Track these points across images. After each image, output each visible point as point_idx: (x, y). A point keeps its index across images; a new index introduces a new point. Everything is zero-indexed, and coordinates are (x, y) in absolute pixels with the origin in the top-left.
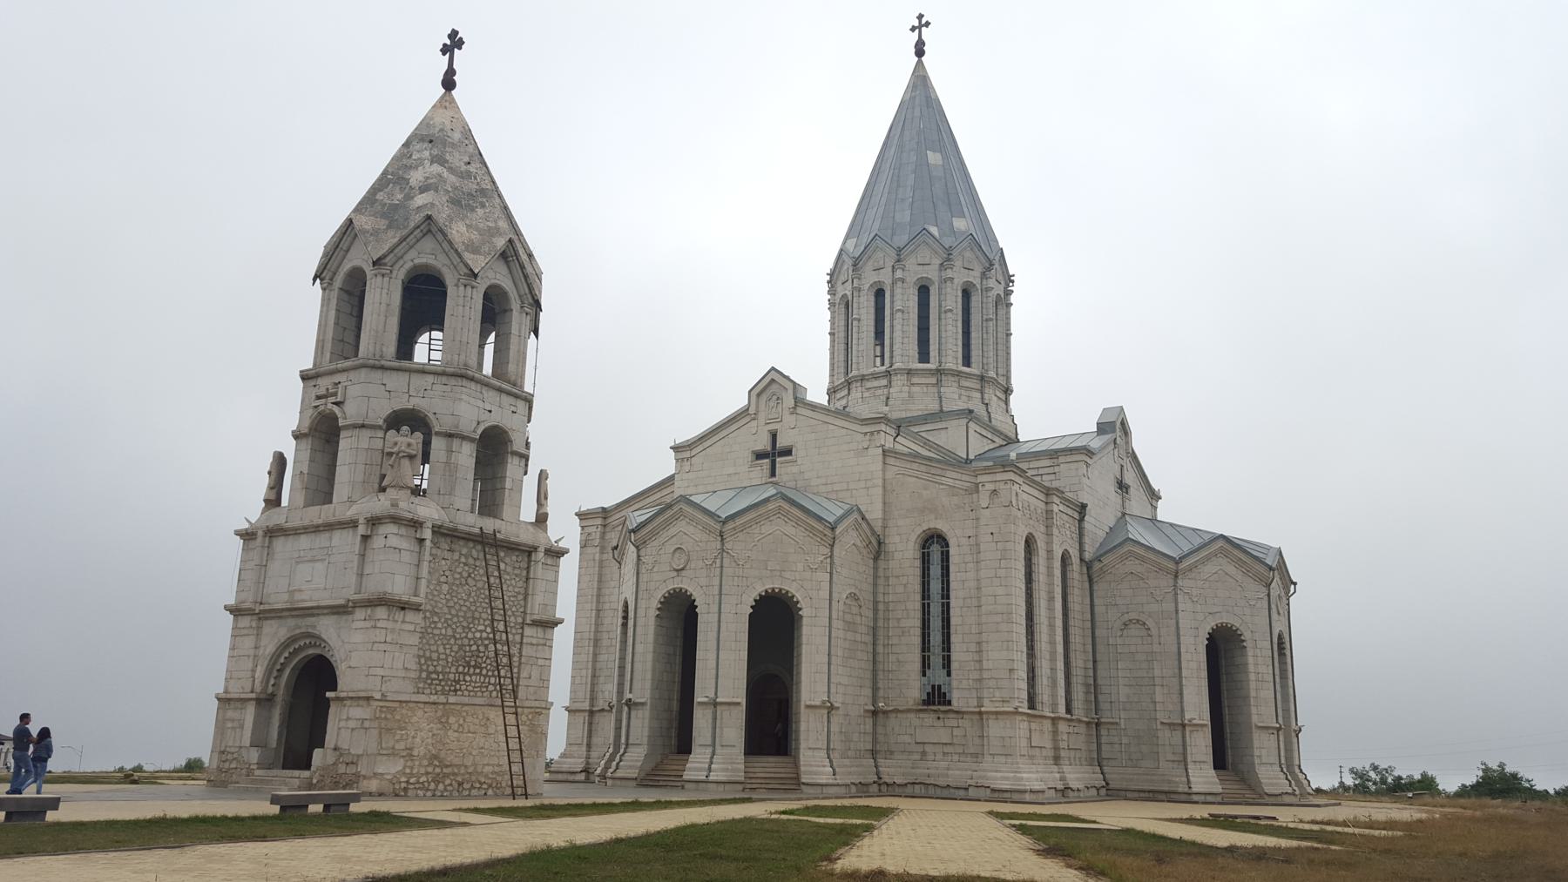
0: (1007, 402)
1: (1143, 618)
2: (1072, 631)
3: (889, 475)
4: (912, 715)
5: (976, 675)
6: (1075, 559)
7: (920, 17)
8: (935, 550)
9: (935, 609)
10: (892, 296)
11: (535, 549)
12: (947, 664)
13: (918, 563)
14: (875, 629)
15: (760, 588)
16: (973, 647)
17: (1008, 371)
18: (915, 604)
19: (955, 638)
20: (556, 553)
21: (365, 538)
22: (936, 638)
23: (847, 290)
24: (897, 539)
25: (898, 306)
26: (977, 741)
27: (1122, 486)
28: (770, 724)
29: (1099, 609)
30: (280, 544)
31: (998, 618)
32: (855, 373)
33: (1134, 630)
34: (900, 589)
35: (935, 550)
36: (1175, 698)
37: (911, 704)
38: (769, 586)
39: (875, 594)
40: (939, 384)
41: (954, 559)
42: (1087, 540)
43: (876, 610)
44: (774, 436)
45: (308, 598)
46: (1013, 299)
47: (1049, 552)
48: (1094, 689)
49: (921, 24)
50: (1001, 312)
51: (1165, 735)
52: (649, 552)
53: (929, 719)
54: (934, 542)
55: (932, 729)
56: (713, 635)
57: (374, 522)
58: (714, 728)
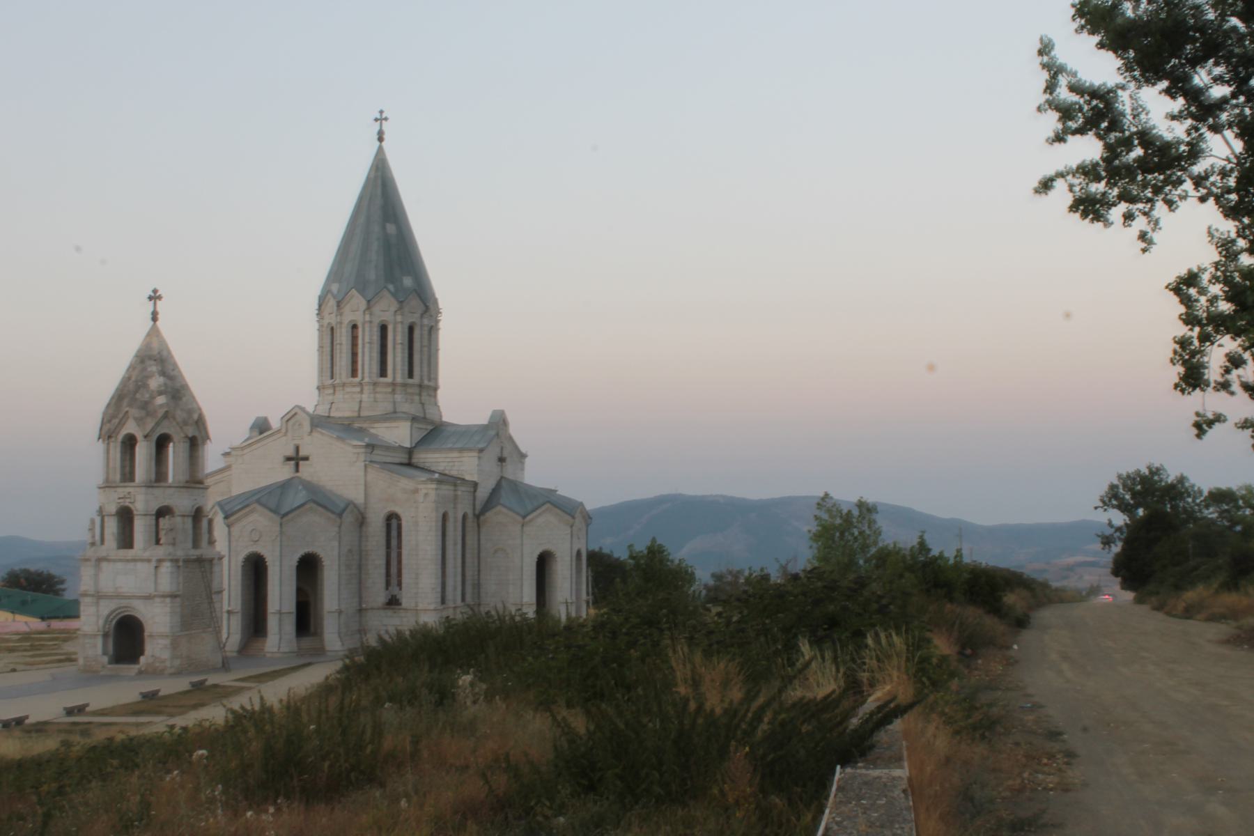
2: (468, 556)
6: (470, 515)
7: (381, 112)
8: (394, 522)
9: (394, 555)
12: (400, 584)
13: (384, 529)
14: (360, 567)
18: (383, 551)
19: (404, 571)
20: (221, 558)
21: (156, 567)
22: (394, 570)
23: (331, 319)
25: (367, 340)
27: (502, 460)
28: (306, 618)
29: (482, 542)
30: (104, 565)
32: (338, 381)
39: (360, 546)
40: (393, 392)
44: (297, 449)
46: (441, 325)
47: (455, 518)
48: (478, 586)
49: (381, 119)
52: (236, 530)
53: (390, 613)
54: (392, 520)
57: (160, 561)
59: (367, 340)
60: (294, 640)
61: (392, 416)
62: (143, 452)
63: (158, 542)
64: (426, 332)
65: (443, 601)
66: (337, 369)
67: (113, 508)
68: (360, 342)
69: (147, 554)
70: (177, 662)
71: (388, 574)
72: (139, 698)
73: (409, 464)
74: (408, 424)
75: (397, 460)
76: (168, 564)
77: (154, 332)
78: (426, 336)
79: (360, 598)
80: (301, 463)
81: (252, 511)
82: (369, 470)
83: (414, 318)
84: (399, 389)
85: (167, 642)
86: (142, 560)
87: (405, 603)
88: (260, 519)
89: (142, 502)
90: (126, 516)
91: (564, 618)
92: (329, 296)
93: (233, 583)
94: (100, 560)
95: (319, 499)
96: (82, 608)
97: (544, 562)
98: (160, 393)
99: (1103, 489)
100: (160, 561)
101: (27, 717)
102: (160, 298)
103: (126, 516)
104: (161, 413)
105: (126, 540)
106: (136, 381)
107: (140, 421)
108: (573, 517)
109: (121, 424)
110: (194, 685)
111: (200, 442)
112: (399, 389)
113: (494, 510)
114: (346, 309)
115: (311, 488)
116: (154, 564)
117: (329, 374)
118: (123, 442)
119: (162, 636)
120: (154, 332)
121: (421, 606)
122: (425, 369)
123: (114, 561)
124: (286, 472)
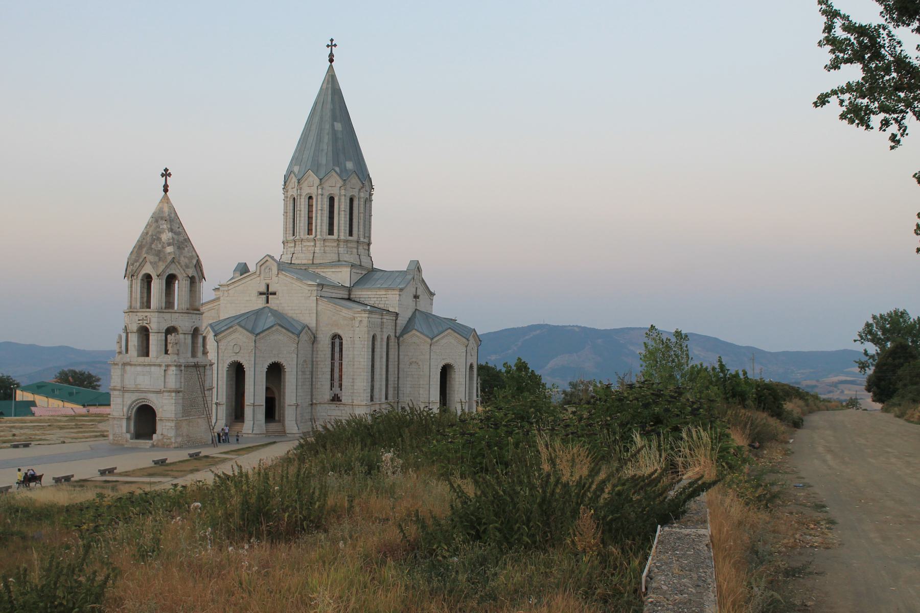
0: (369, 250)
3: (319, 309)
6: (393, 337)
7: (332, 40)
8: (337, 341)
9: (337, 364)
12: (341, 386)
13: (330, 346)
14: (312, 372)
15: (270, 361)
17: (370, 234)
20: (211, 365)
22: (336, 375)
23: (293, 192)
25: (319, 208)
27: (416, 297)
28: (272, 410)
29: (401, 357)
30: (128, 368)
38: (273, 360)
40: (338, 245)
41: (344, 346)
42: (398, 328)
43: (312, 365)
46: (373, 197)
49: (332, 45)
50: (368, 205)
52: (222, 344)
53: (333, 406)
54: (336, 337)
56: (252, 380)
57: (167, 366)
59: (319, 208)
60: (264, 425)
61: (338, 263)
62: (157, 287)
63: (166, 352)
64: (362, 203)
65: (372, 400)
66: (297, 228)
67: (134, 327)
68: (314, 209)
69: (158, 361)
70: (179, 439)
71: (332, 379)
72: (153, 464)
73: (349, 299)
74: (349, 269)
75: (340, 296)
76: (174, 368)
77: (166, 199)
78: (362, 206)
79: (312, 395)
80: (270, 296)
81: (234, 331)
82: (320, 302)
83: (355, 192)
84: (342, 244)
85: (173, 424)
86: (154, 365)
88: (241, 337)
89: (156, 323)
90: (144, 332)
91: (459, 413)
92: (292, 175)
93: (220, 383)
94: (124, 364)
95: (284, 323)
97: (446, 371)
98: (169, 245)
99: (861, 327)
101: (73, 476)
102: (170, 175)
103: (144, 332)
104: (169, 258)
106: (152, 235)
107: (154, 264)
108: (468, 340)
109: (141, 266)
110: (191, 455)
111: (197, 280)
113: (411, 333)
114: (305, 185)
115: (275, 313)
116: (163, 368)
117: (291, 232)
118: (142, 280)
120: (166, 199)
121: (355, 402)
122: (361, 230)
123: (135, 365)
124: (260, 303)
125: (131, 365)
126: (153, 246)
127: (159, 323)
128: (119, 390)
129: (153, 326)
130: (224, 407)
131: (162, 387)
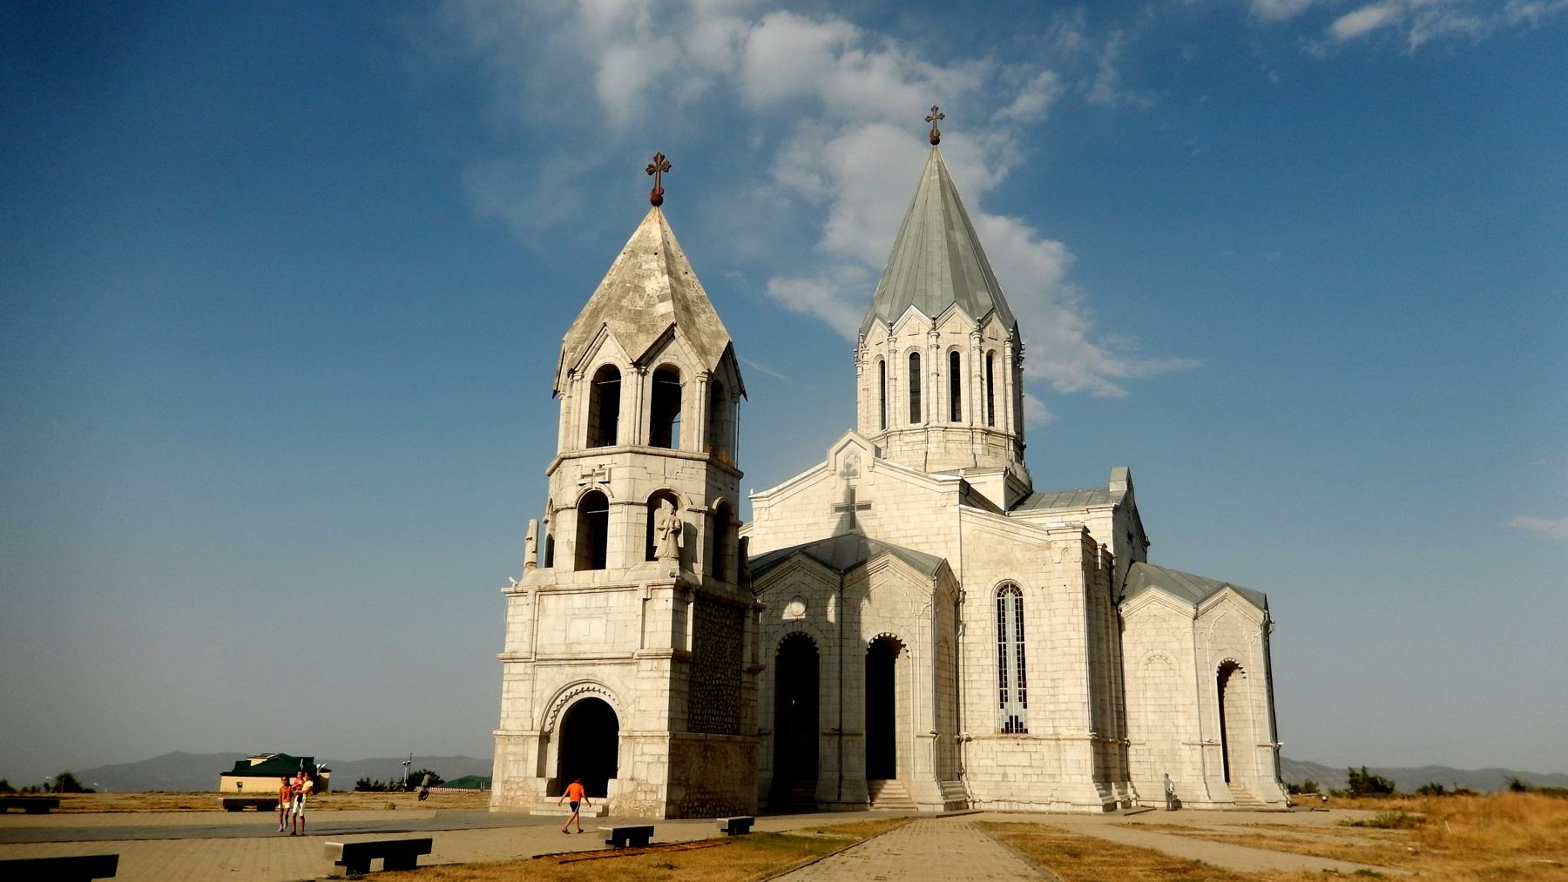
1: (1166, 653)
4: (993, 742)
5: (1051, 708)
8: (1010, 598)
10: (927, 360)
11: (747, 606)
12: (1023, 697)
16: (1048, 683)
18: (992, 644)
24: (974, 588)
26: (1055, 764)
30: (550, 601)
31: (1073, 659)
33: (1158, 664)
34: (979, 632)
35: (1010, 598)
36: (1195, 722)
37: (992, 731)
45: (586, 650)
51: (1186, 752)
53: (1009, 743)
54: (1009, 589)
55: (1011, 752)
57: (654, 587)
58: (840, 756)
69: (627, 580)
70: (680, 795)
85: (664, 749)
86: (619, 588)
87: (1033, 727)
94: (542, 591)
96: (505, 684)
98: (662, 299)
100: (654, 587)
102: (667, 168)
105: (592, 552)
106: (624, 282)
109: (593, 347)
111: (727, 396)
112: (978, 437)
116: (642, 594)
117: (878, 423)
119: (651, 737)
121: (1064, 732)
123: (569, 592)
125: (555, 591)
126: (624, 302)
127: (633, 479)
128: (526, 660)
129: (617, 491)
130: (771, 738)
131: (633, 647)
